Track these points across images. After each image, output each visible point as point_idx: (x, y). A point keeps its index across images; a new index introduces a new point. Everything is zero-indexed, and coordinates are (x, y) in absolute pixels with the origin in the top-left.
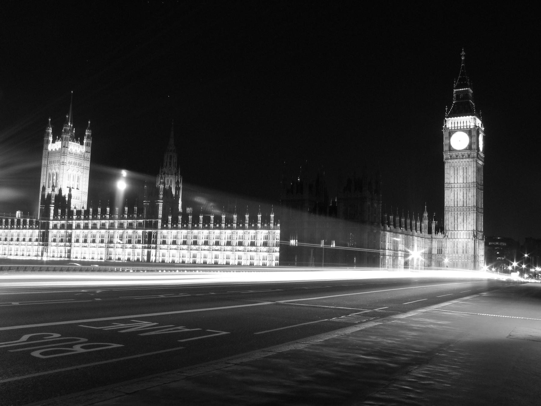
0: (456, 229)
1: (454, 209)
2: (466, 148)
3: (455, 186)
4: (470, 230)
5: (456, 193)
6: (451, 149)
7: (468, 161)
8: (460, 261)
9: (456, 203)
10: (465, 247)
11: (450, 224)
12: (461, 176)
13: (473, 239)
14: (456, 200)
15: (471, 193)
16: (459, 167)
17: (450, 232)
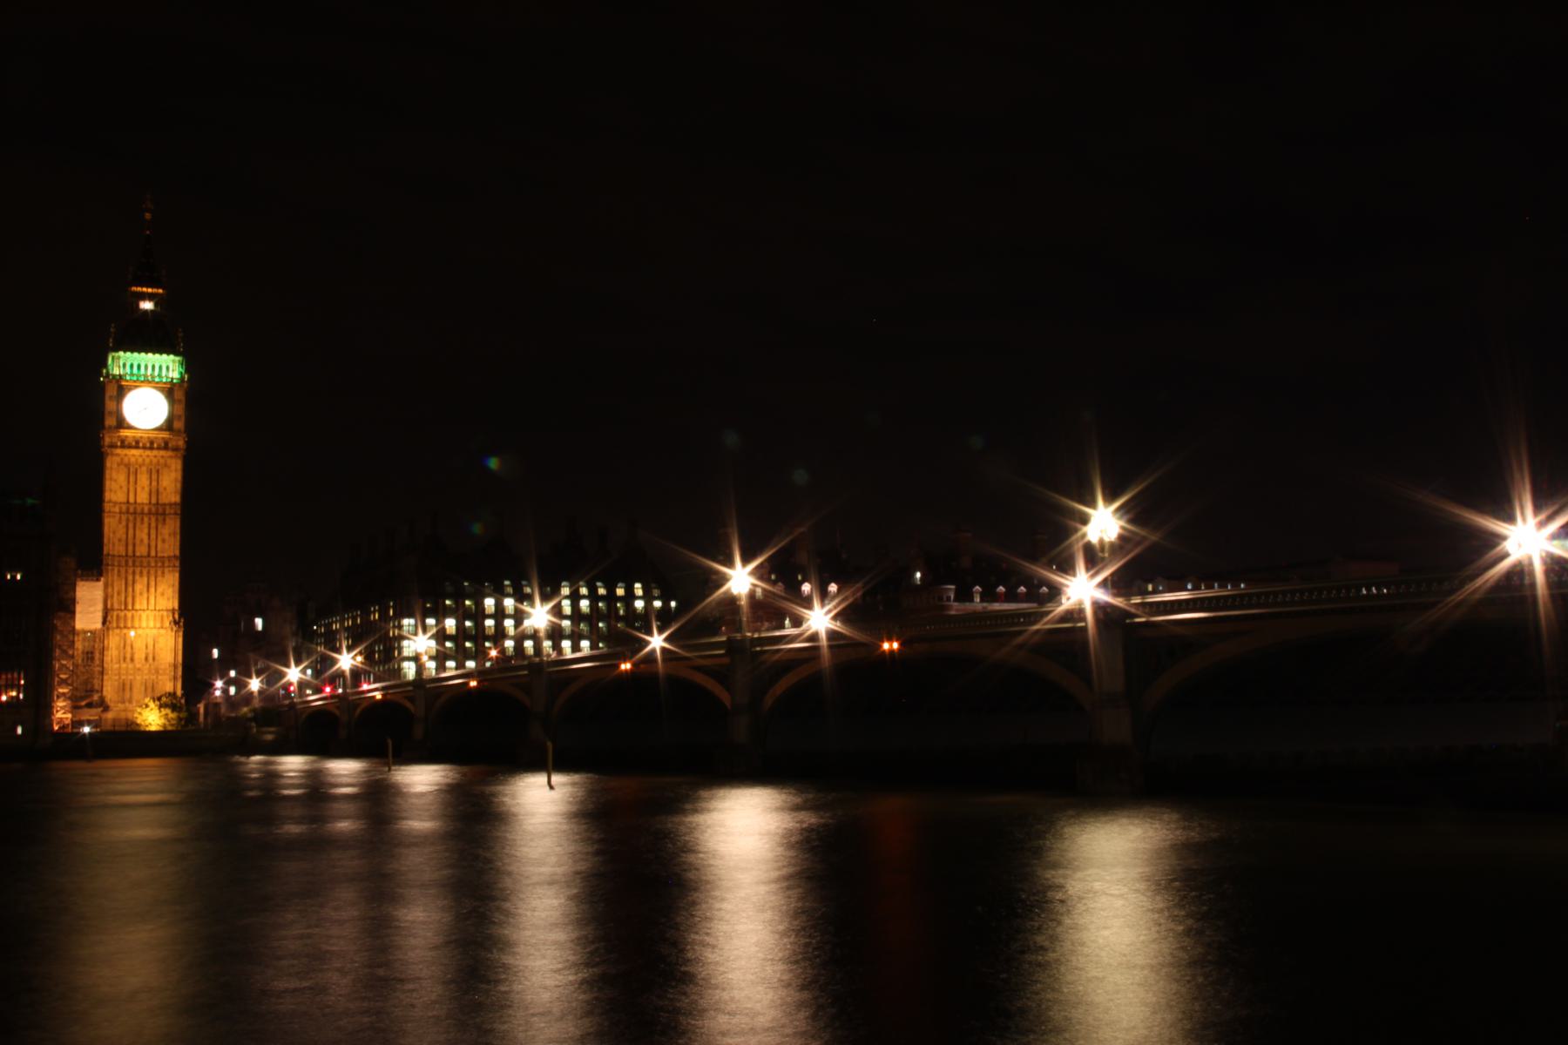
0: (130, 607)
1: (127, 562)
2: (162, 425)
3: (128, 509)
4: (162, 610)
5: (131, 525)
6: (121, 423)
7: (162, 457)
8: (138, 678)
9: (130, 548)
10: (152, 647)
11: (115, 595)
12: (143, 488)
13: (172, 629)
14: (130, 541)
15: (167, 527)
16: (140, 466)
17: (115, 613)
